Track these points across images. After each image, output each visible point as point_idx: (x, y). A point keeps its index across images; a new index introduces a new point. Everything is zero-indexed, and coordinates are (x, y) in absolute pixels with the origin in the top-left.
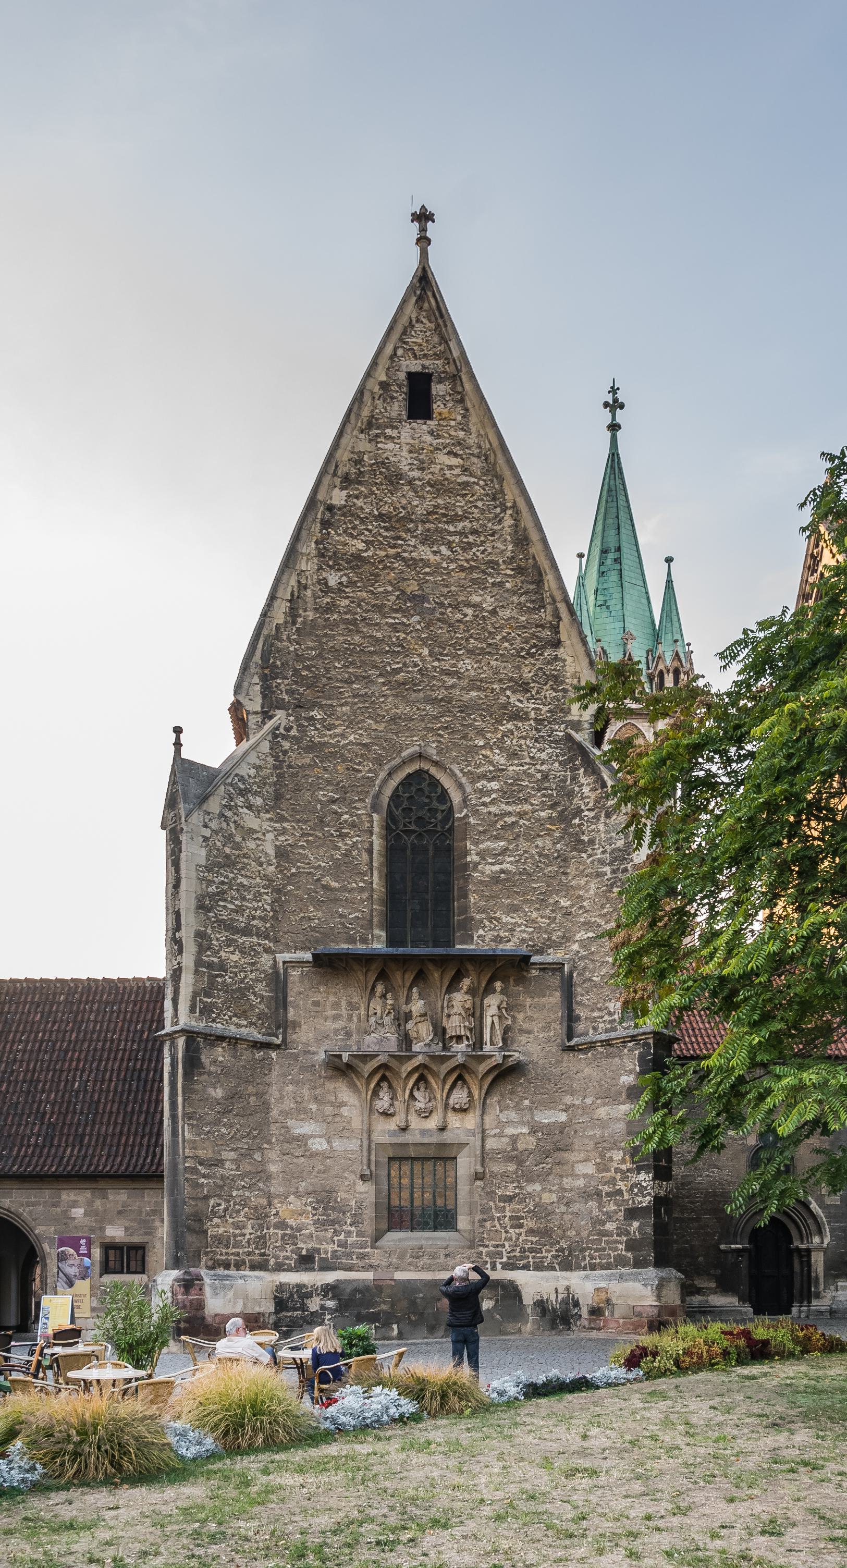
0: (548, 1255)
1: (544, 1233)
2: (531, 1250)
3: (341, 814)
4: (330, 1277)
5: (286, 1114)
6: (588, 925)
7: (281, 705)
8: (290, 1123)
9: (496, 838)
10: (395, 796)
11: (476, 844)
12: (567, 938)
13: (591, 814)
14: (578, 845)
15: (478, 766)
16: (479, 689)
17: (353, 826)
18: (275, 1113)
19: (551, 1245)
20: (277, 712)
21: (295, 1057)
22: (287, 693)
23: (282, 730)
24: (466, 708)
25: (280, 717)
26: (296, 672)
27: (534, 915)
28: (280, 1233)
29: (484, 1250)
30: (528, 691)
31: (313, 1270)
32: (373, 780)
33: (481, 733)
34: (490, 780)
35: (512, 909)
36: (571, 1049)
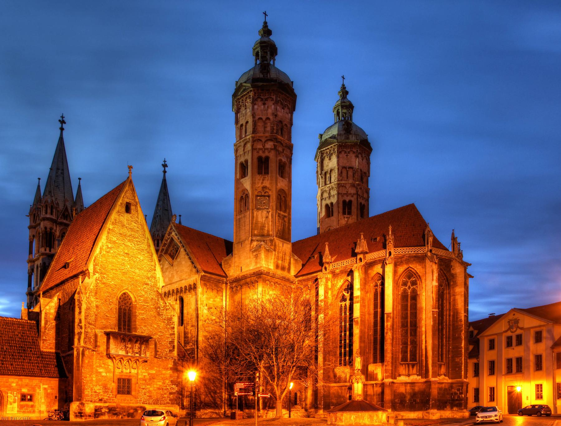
0: (151, 401)
1: (150, 396)
2: (147, 400)
3: (110, 300)
4: (107, 405)
5: (97, 366)
6: (160, 332)
7: (97, 272)
8: (98, 369)
9: (142, 310)
10: (120, 298)
11: (138, 310)
12: (156, 334)
13: (162, 309)
14: (159, 314)
15: (139, 294)
16: (140, 277)
17: (112, 303)
18: (94, 366)
19: (152, 399)
20: (96, 274)
21: (99, 354)
22: (99, 269)
23: (97, 278)
24: (136, 281)
25: (97, 275)
26: (101, 265)
27: (149, 328)
28: (95, 394)
29: (138, 399)
30: (149, 279)
31: (102, 402)
32: (117, 293)
33: (140, 286)
34: (141, 297)
35: (145, 326)
36: (157, 358)
